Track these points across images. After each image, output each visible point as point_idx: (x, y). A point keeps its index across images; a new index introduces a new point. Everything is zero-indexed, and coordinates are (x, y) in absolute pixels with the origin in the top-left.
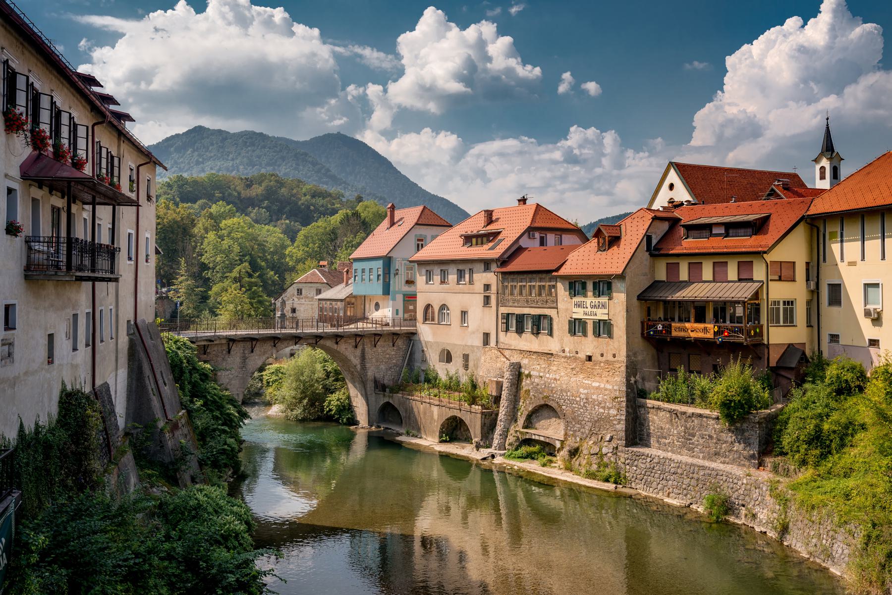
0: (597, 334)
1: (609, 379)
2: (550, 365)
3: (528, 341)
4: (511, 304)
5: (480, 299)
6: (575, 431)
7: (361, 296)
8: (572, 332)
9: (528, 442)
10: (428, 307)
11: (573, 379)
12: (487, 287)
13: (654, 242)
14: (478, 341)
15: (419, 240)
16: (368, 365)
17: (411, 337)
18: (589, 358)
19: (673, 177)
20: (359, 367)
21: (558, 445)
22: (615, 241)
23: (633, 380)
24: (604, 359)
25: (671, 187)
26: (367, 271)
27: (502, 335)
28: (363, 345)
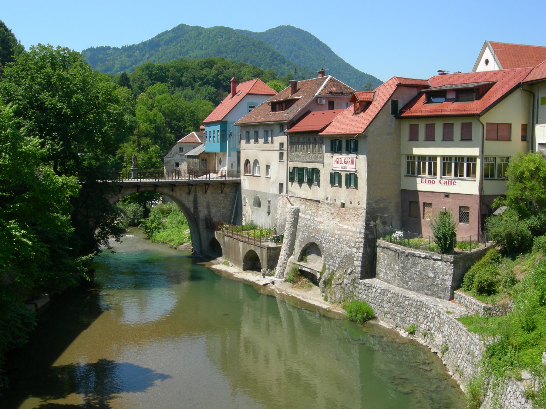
0: (348, 185)
1: (355, 222)
2: (317, 210)
3: (304, 191)
4: (296, 159)
5: (277, 154)
6: (329, 265)
7: (212, 153)
8: (332, 183)
9: (302, 273)
10: (247, 162)
11: (332, 223)
12: (282, 145)
13: (400, 106)
14: (276, 191)
15: (250, 107)
16: (200, 208)
17: (237, 185)
18: (343, 205)
19: (488, 54)
20: (192, 210)
21: (318, 276)
22: (366, 105)
23: (372, 224)
24: (352, 205)
25: (487, 62)
26: (212, 132)
27: (290, 184)
28: (196, 192)
